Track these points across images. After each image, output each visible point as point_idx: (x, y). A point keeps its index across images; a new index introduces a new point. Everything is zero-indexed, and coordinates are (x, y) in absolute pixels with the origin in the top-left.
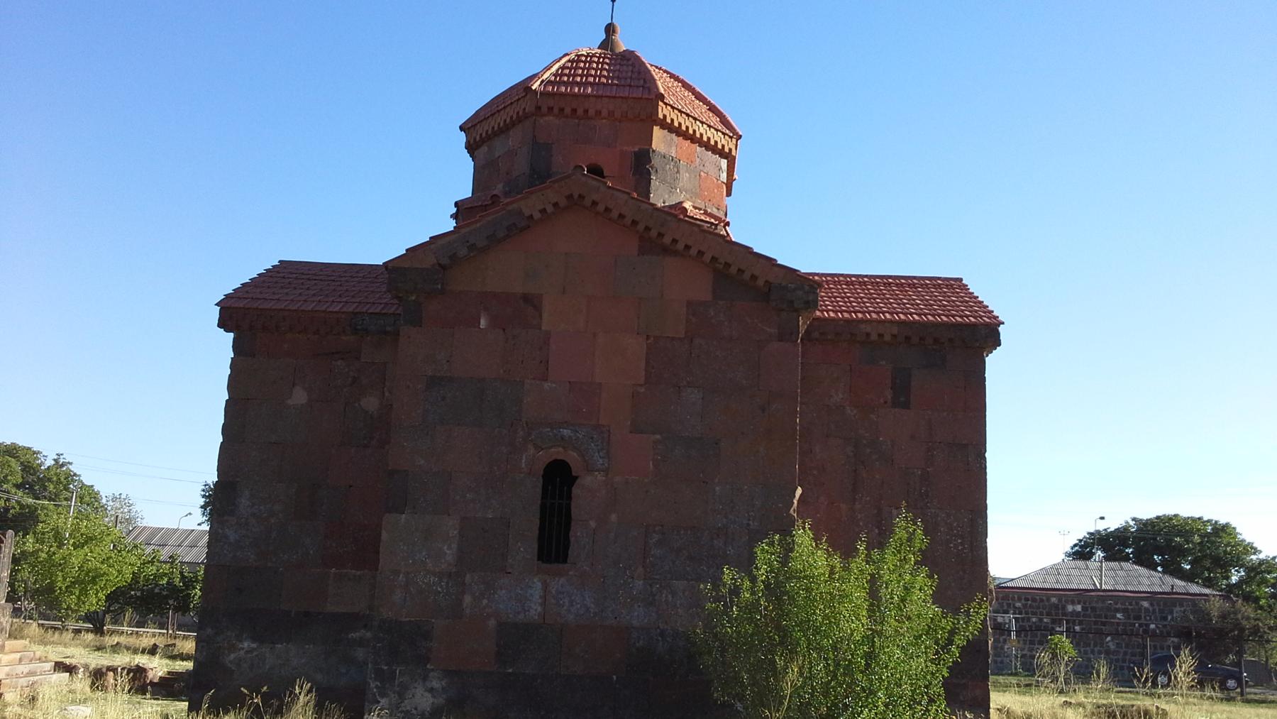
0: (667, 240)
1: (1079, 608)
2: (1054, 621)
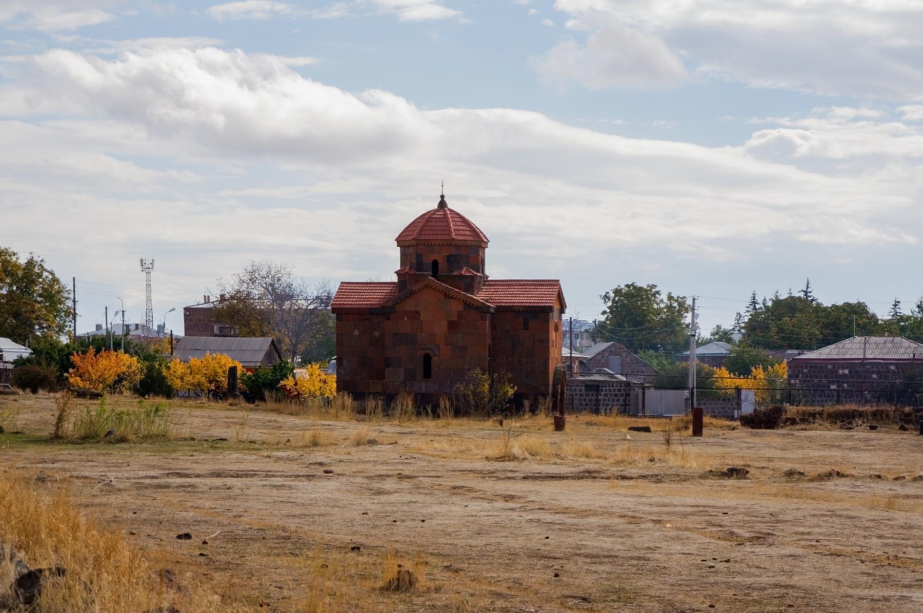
1: (847, 372)
2: (829, 382)
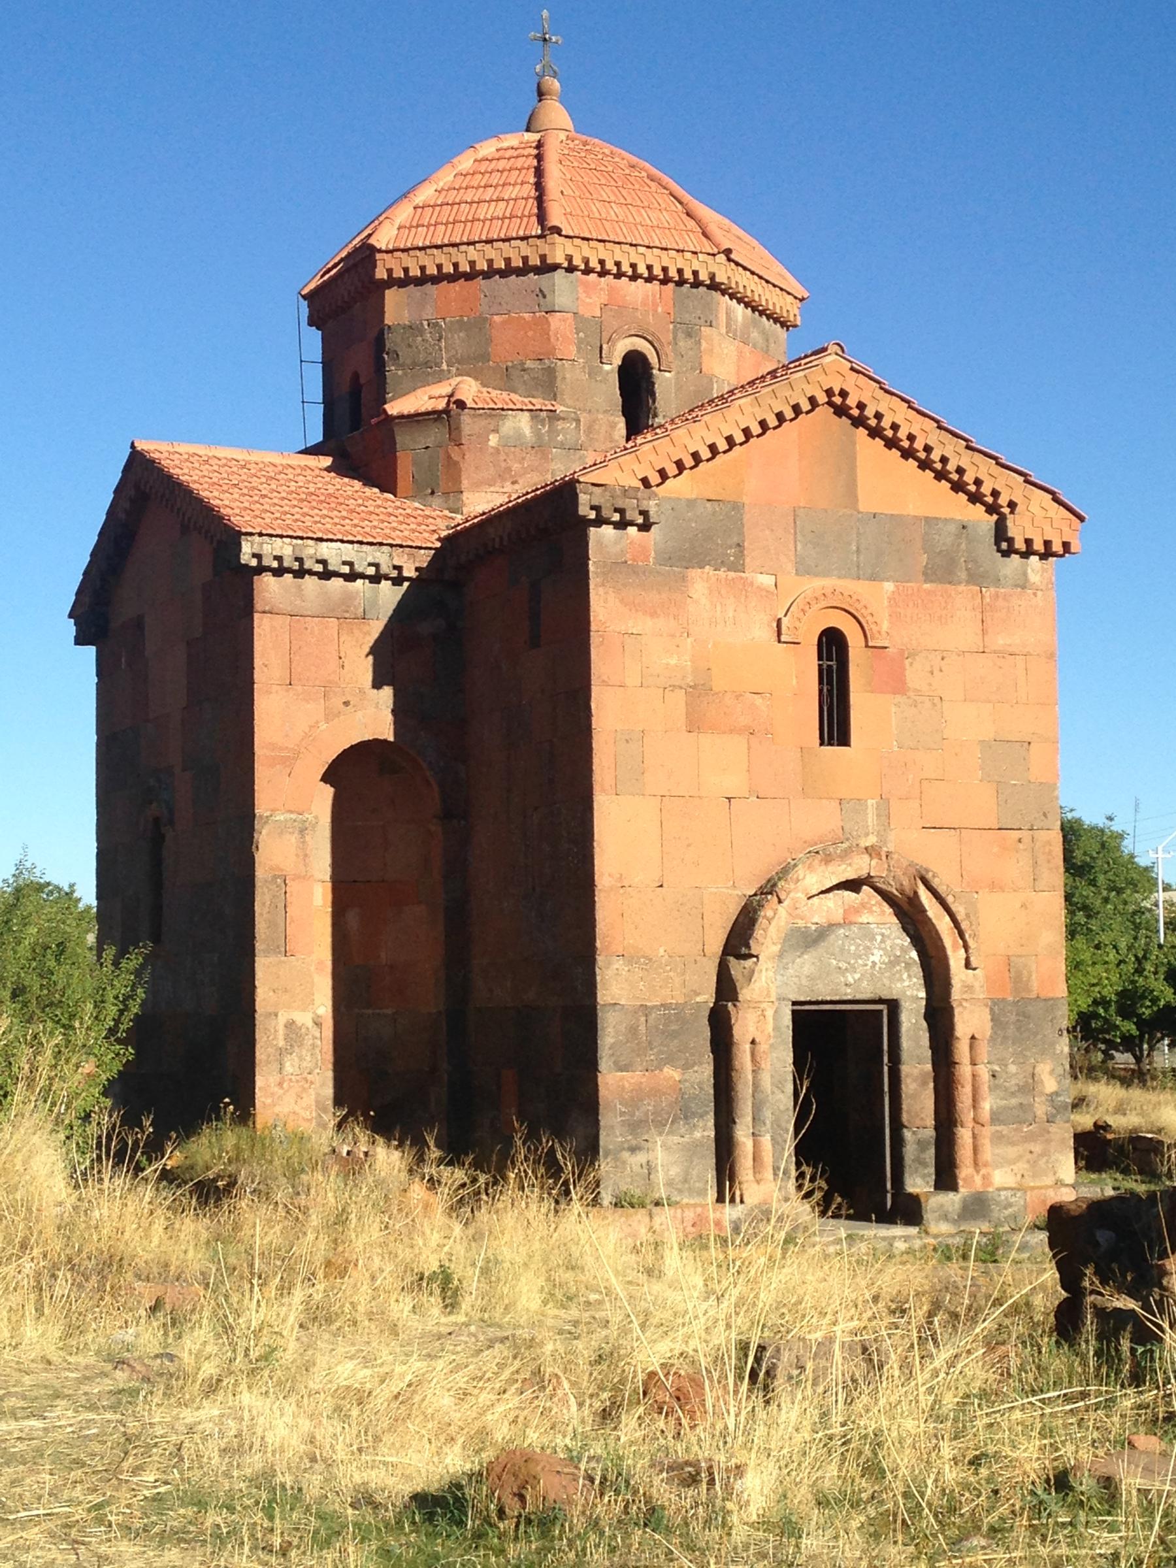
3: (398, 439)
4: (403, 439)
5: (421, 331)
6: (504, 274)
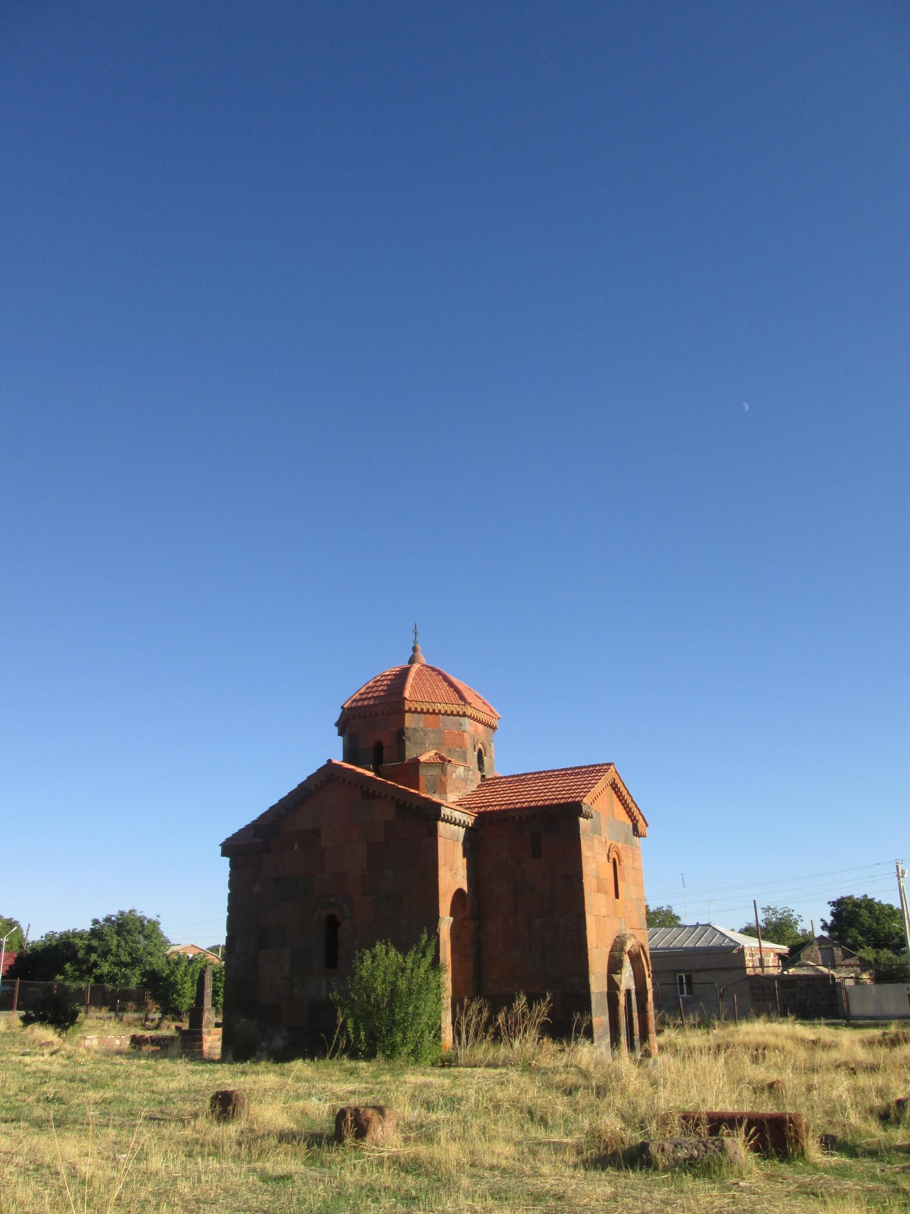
0: (371, 791)
3: (421, 771)
4: (422, 771)
5: (418, 731)
6: (448, 715)
